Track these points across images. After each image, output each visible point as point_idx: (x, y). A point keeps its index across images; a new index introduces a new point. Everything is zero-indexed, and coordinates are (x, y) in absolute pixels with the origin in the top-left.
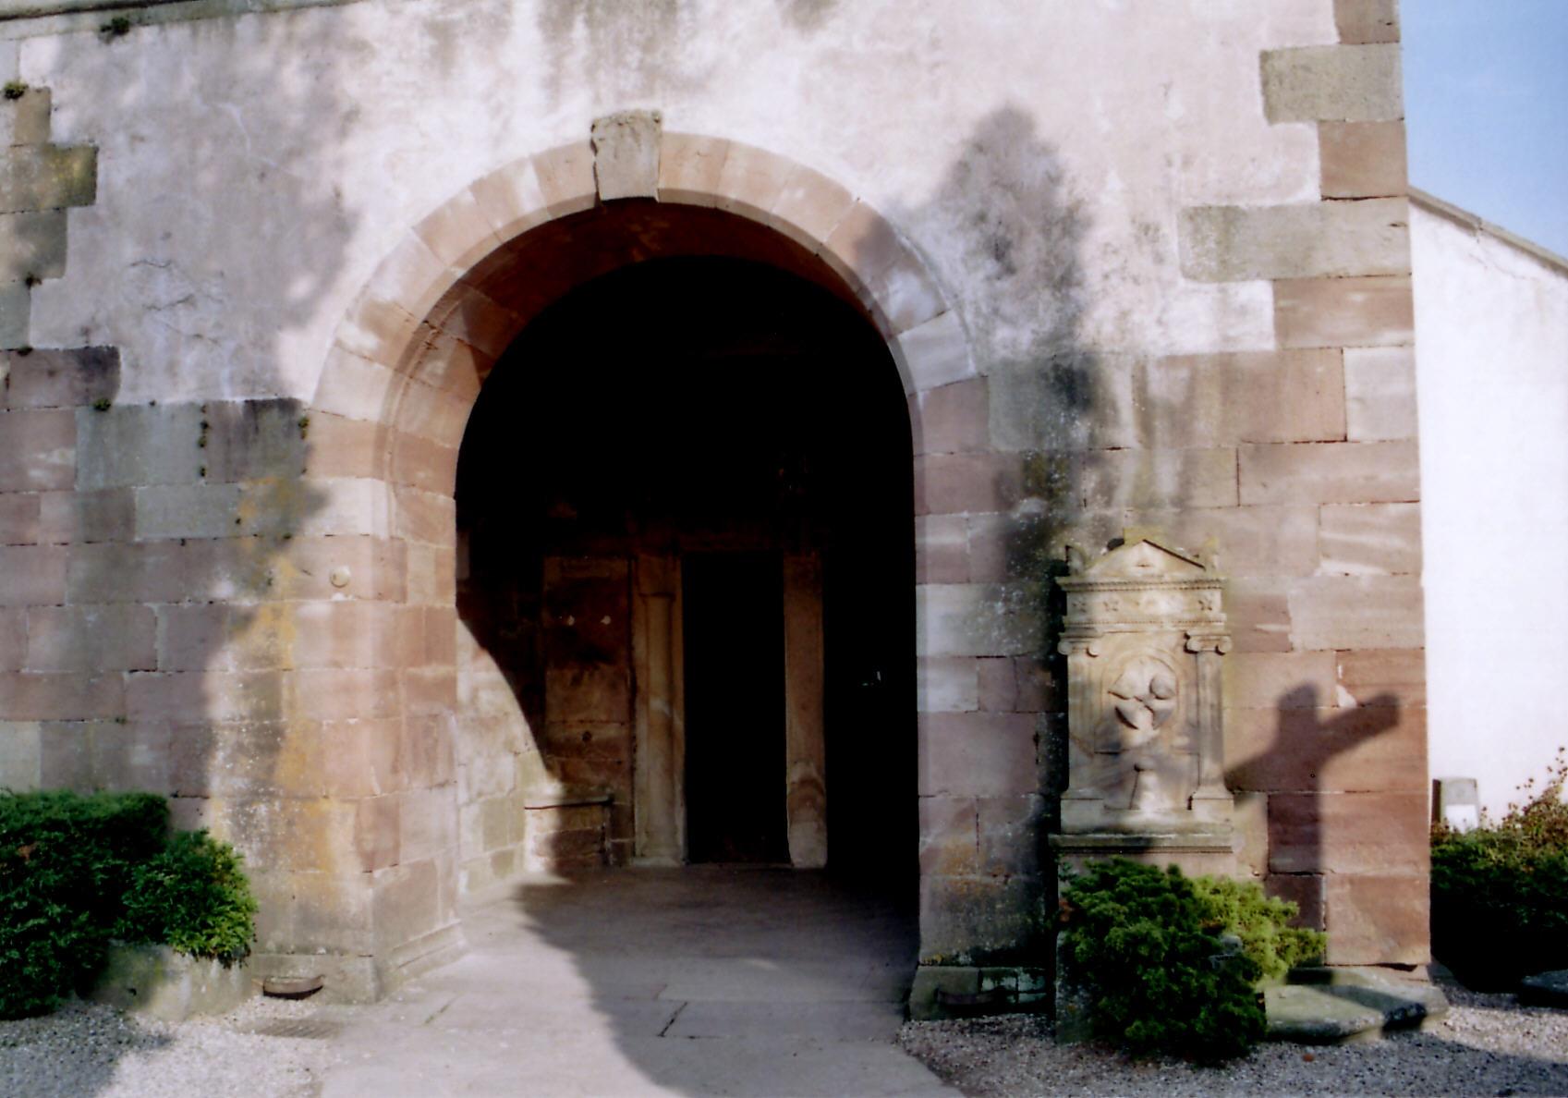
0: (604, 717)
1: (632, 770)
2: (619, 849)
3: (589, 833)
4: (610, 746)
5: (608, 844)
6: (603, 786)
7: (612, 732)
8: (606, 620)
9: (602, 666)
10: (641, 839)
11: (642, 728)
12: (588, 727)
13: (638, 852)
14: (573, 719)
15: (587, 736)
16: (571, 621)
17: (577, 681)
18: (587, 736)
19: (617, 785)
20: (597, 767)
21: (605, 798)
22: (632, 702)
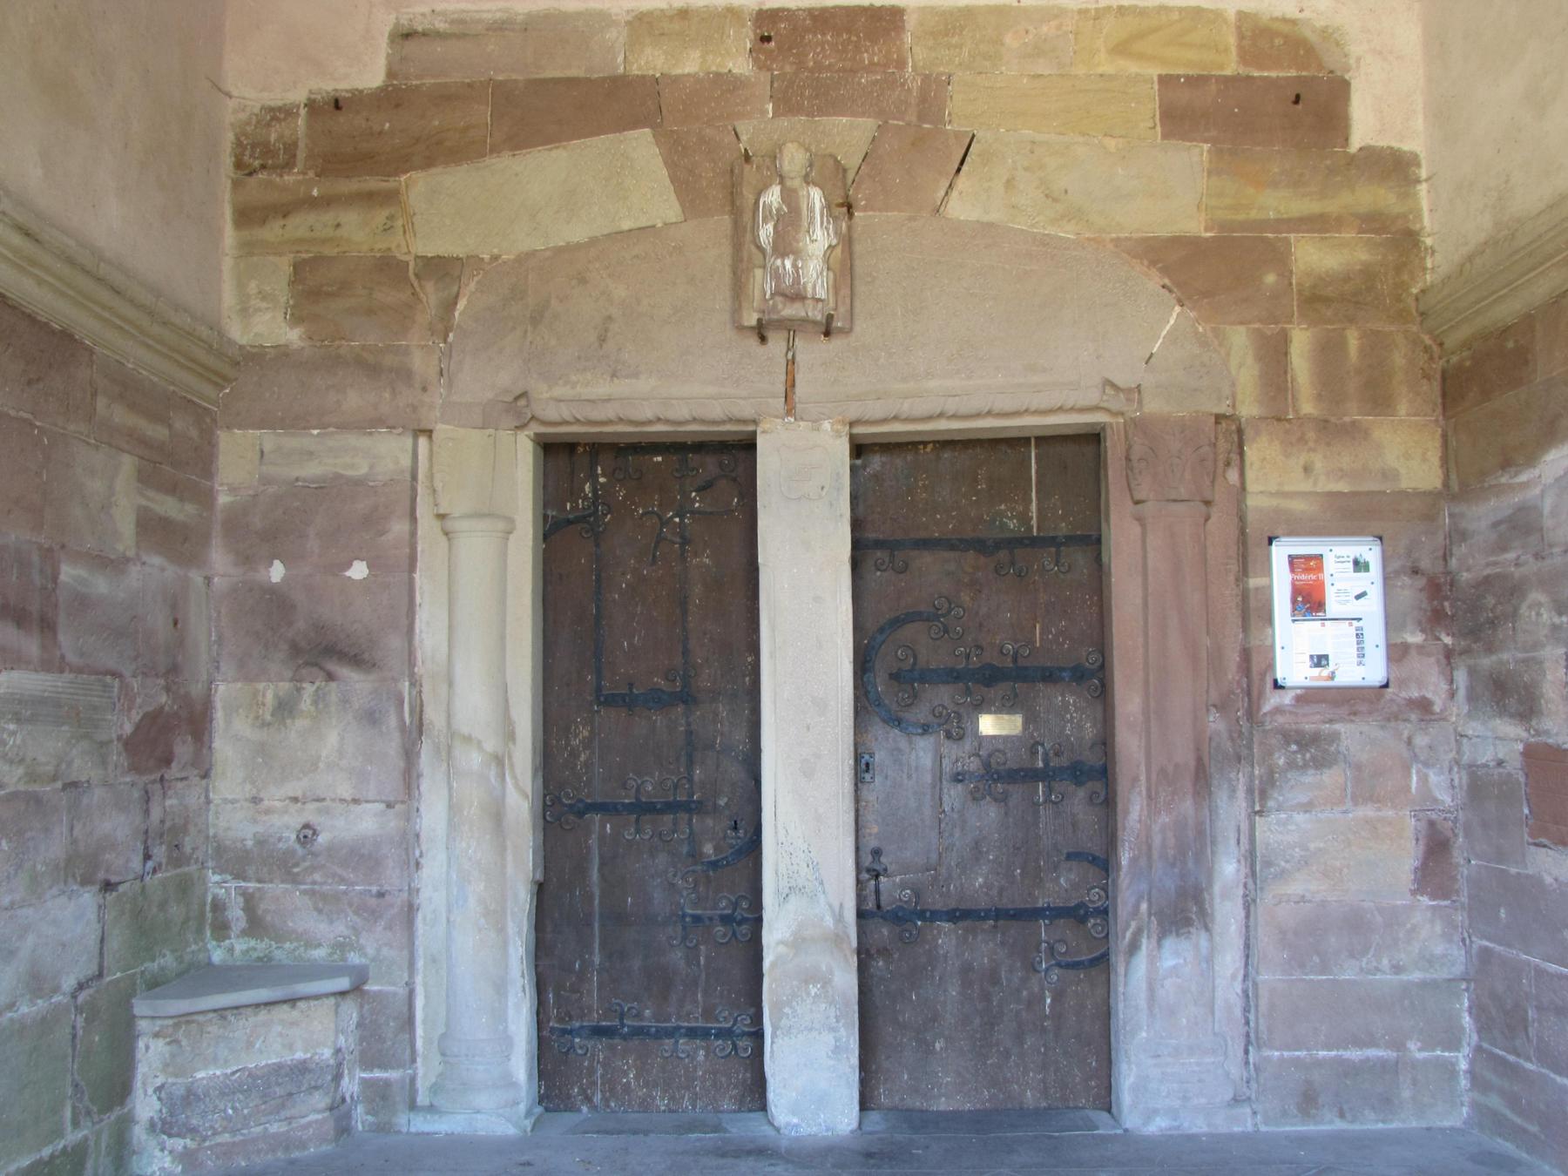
0: (345, 791)
1: (411, 910)
2: (378, 1095)
3: (302, 1068)
4: (362, 858)
5: (350, 1087)
6: (341, 947)
7: (366, 822)
8: (358, 571)
9: (344, 672)
10: (426, 1072)
11: (433, 815)
12: (310, 814)
13: (422, 1099)
14: (274, 796)
15: (307, 834)
16: (277, 572)
17: (285, 709)
18: (307, 834)
19: (373, 945)
20: (326, 903)
21: (343, 983)
22: (410, 755)
